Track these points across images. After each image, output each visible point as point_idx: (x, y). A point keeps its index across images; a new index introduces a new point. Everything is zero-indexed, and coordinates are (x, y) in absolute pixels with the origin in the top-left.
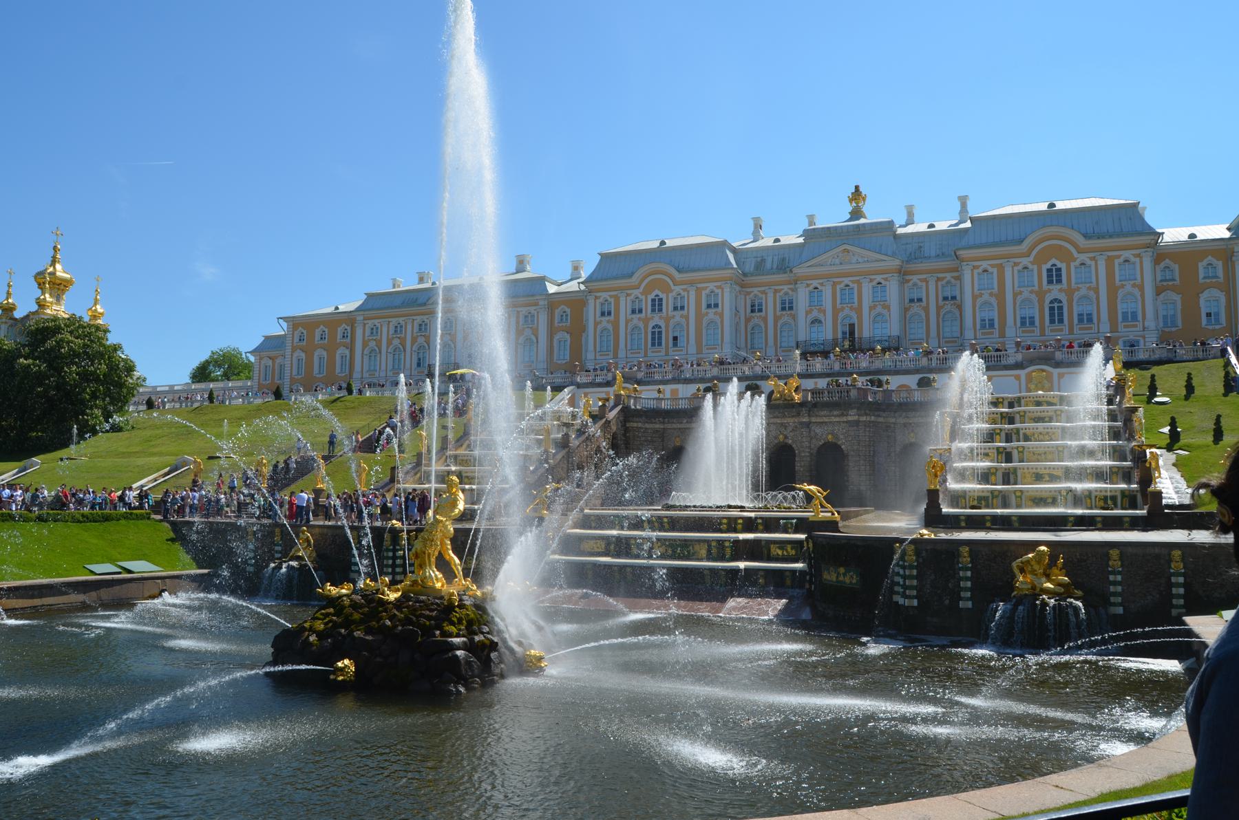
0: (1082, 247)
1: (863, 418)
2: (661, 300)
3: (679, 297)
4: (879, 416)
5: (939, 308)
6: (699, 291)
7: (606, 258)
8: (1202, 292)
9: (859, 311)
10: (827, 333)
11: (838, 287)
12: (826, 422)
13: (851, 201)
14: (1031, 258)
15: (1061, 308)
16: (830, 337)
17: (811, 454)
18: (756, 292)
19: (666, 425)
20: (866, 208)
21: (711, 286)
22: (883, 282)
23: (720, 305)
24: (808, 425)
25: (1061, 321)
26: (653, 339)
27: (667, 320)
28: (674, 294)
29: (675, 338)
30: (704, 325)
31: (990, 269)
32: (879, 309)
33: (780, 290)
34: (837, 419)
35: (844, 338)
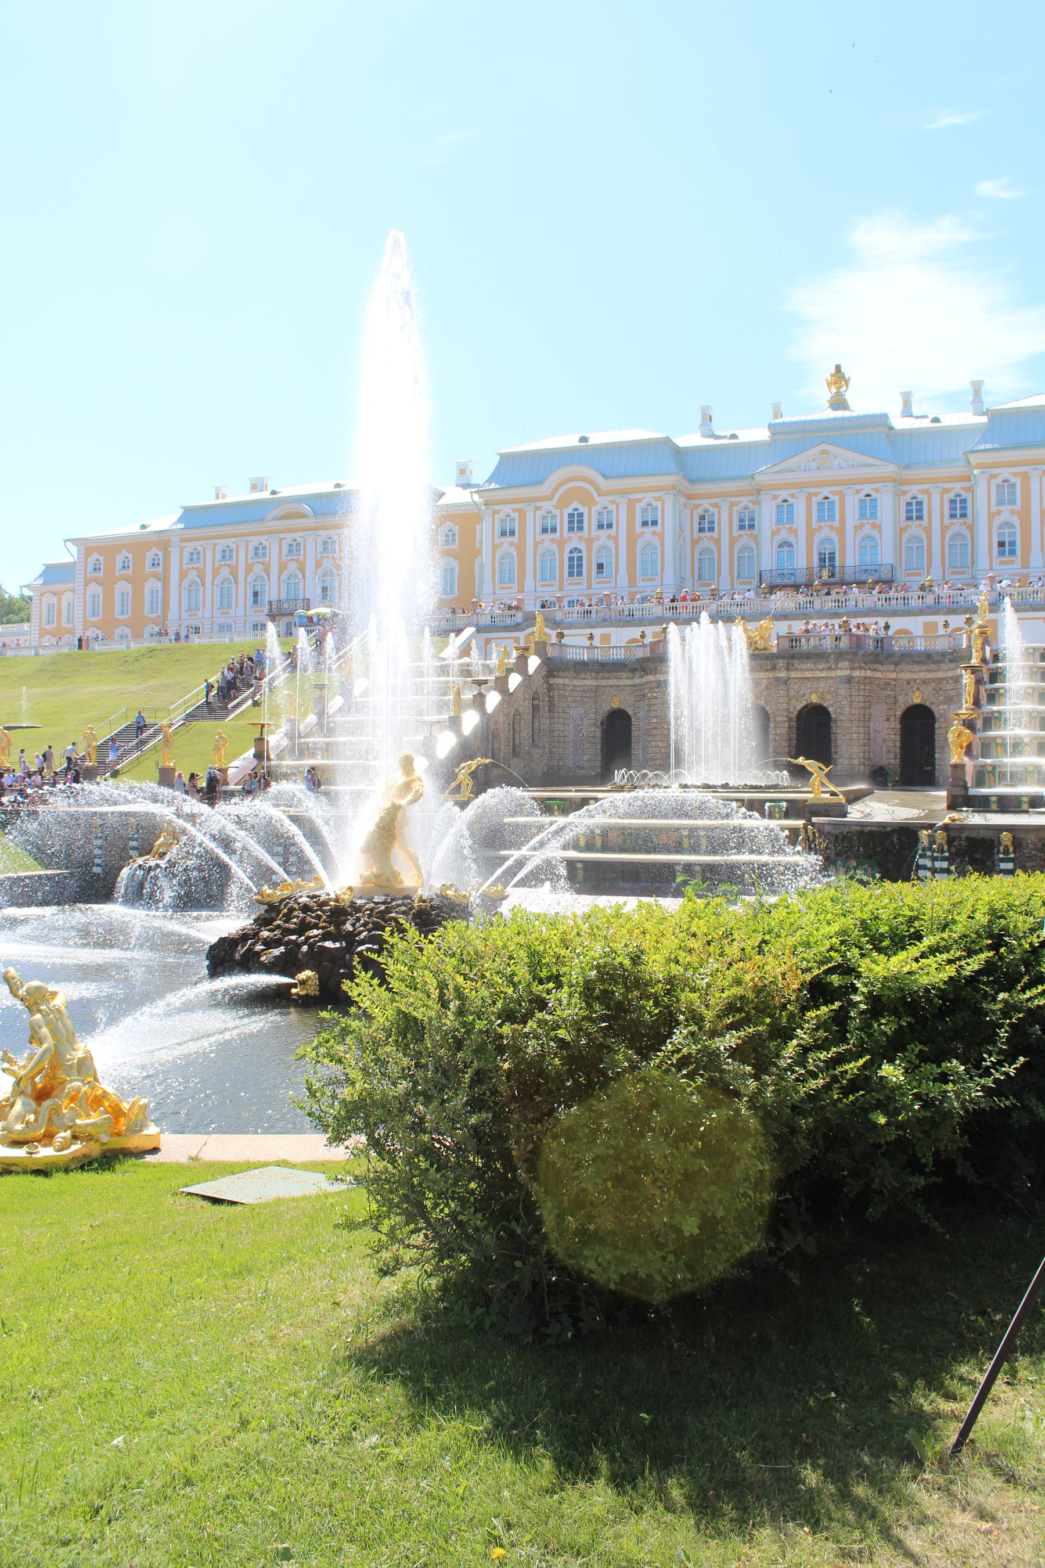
1: (857, 673)
2: (581, 515)
3: (605, 511)
4: (875, 670)
5: (944, 529)
6: (631, 504)
7: (508, 461)
9: (841, 531)
10: (801, 560)
11: (815, 500)
12: (808, 679)
13: (828, 384)
17: (790, 719)
19: (595, 683)
20: (850, 395)
21: (648, 497)
22: (874, 495)
24: (786, 681)
26: (571, 567)
27: (589, 542)
29: (600, 566)
31: (1012, 480)
32: (867, 530)
33: (737, 503)
34: (823, 674)
35: (822, 567)
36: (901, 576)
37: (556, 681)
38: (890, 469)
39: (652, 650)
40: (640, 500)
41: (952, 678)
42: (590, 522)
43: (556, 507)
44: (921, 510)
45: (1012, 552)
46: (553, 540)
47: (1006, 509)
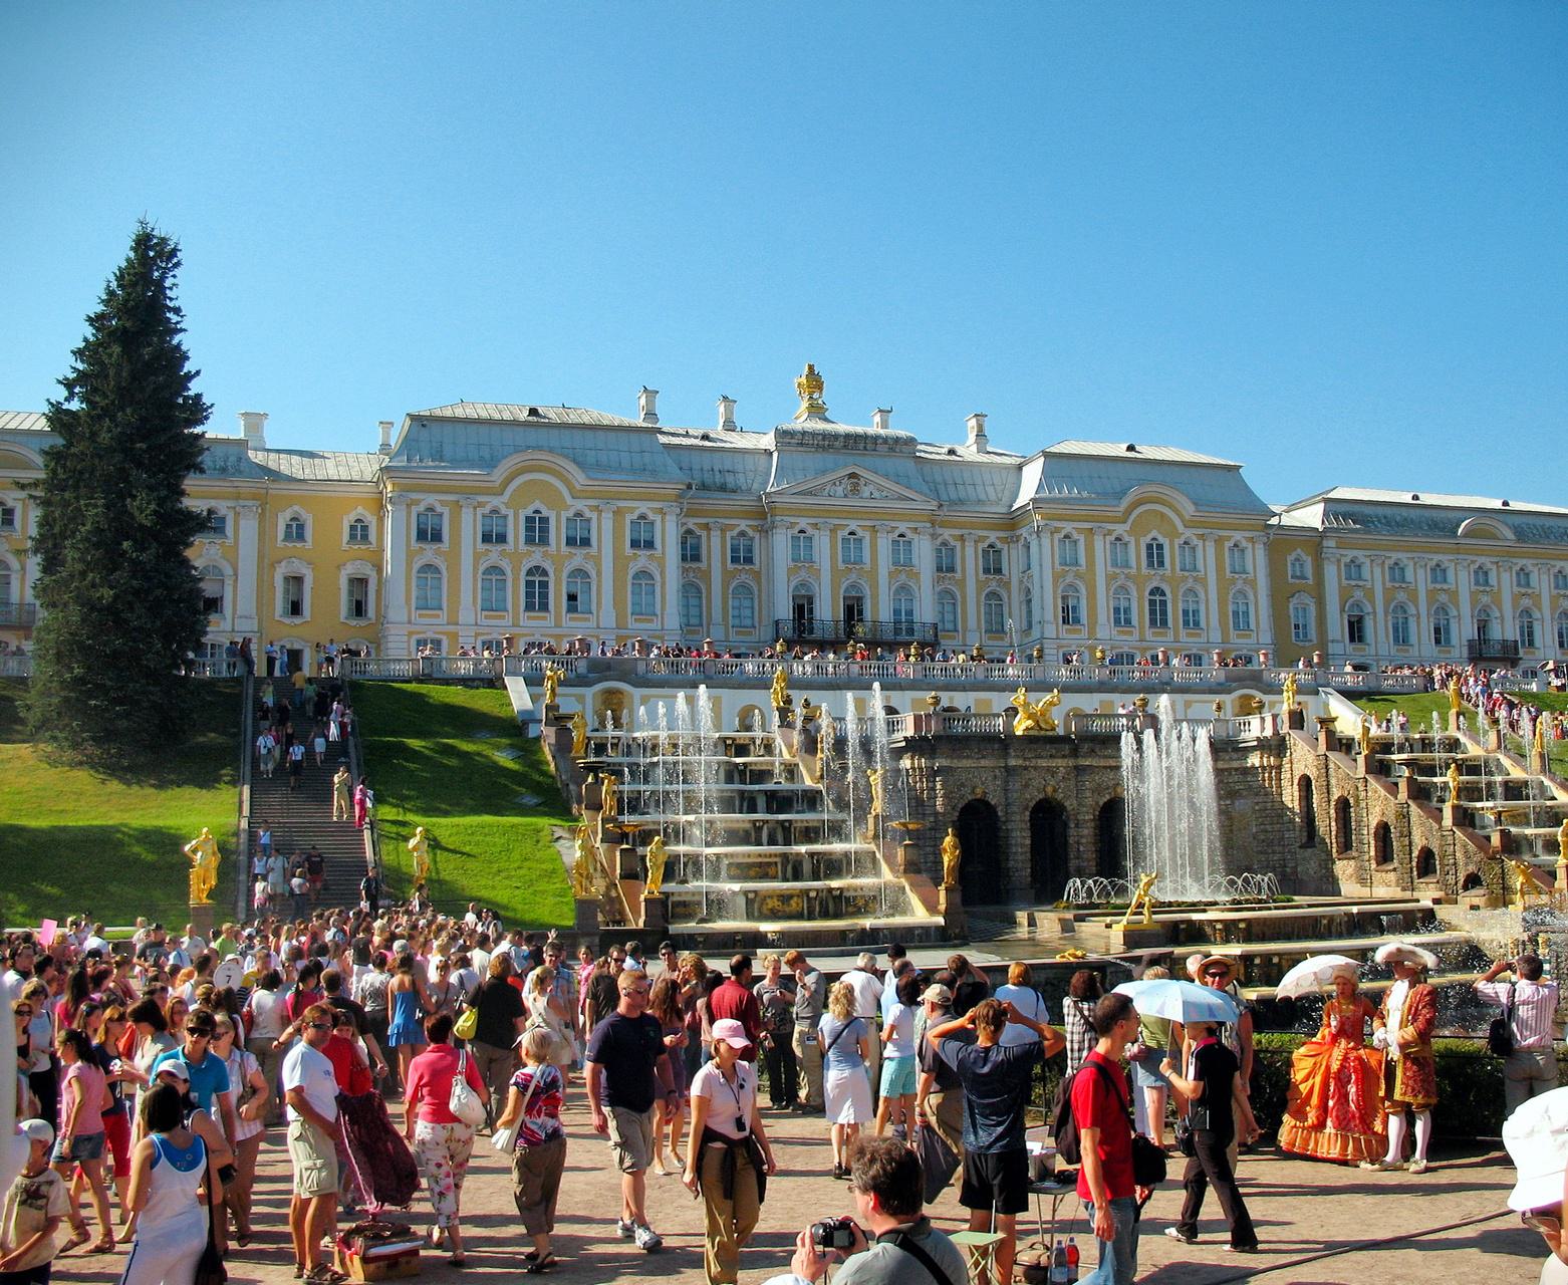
0: (1187, 518)
2: (544, 521)
5: (980, 585)
6: (618, 513)
8: (1292, 596)
14: (1127, 527)
15: (1164, 603)
18: (691, 526)
21: (643, 507)
23: (658, 543)
25: (1164, 623)
26: (529, 595)
28: (570, 514)
29: (572, 598)
30: (631, 573)
31: (1075, 536)
41: (1236, 769)
42: (557, 533)
43: (507, 505)
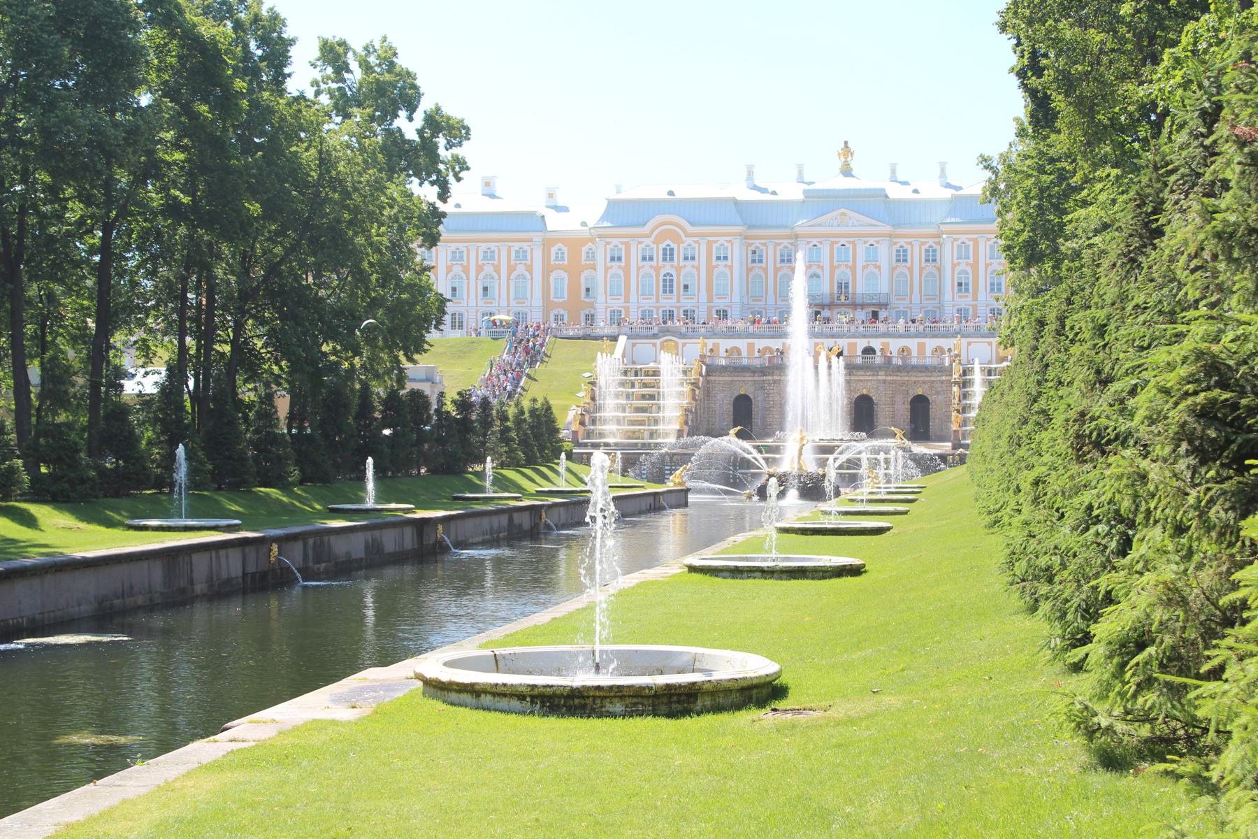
1: (889, 378)
2: (672, 249)
5: (921, 269)
6: (709, 244)
9: (853, 269)
13: (839, 154)
16: (826, 290)
21: (722, 240)
23: (729, 258)
26: (665, 286)
27: (679, 269)
28: (685, 245)
29: (686, 287)
31: (968, 243)
32: (871, 268)
33: (779, 244)
36: (894, 301)
37: (712, 378)
38: (887, 229)
39: (769, 361)
40: (716, 242)
43: (653, 242)
44: (906, 256)
45: (967, 290)
46: (651, 267)
47: (963, 261)
